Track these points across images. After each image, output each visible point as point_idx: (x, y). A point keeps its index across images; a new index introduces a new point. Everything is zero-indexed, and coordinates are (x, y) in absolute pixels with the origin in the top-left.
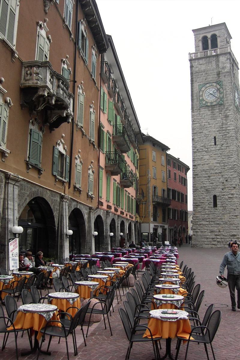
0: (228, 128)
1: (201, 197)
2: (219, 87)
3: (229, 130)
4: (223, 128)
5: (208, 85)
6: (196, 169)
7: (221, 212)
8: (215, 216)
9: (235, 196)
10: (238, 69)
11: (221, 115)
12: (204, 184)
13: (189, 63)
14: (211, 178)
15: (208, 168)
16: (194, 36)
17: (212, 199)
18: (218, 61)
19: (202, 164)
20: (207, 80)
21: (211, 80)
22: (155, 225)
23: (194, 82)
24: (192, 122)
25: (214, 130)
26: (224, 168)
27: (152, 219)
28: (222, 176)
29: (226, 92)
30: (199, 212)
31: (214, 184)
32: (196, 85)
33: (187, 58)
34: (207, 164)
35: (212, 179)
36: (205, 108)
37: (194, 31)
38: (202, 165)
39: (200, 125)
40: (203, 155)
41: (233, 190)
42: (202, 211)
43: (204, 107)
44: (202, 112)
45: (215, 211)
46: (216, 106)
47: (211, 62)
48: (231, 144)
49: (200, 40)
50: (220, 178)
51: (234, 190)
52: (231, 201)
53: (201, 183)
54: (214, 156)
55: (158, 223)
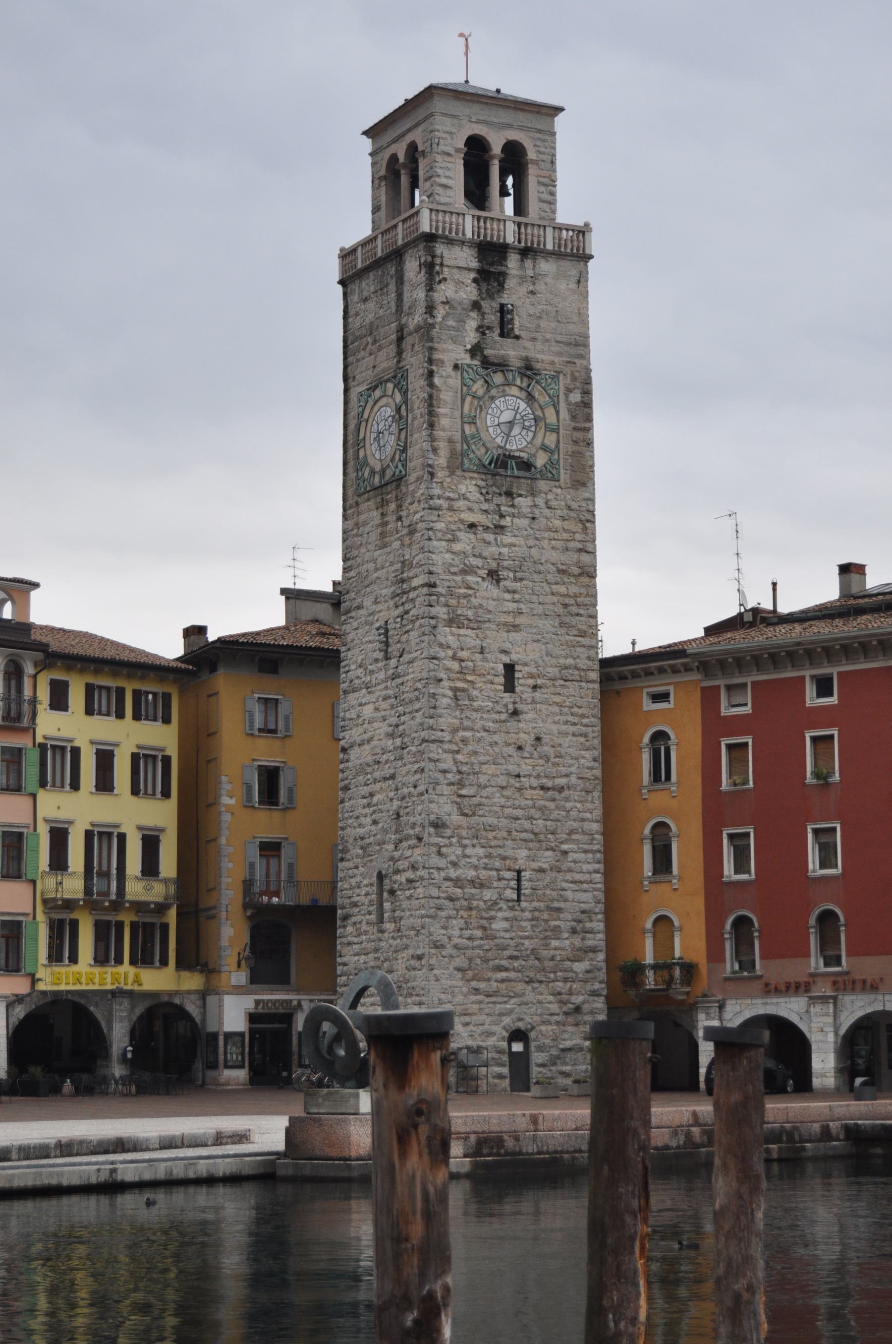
0: (416, 582)
1: (353, 881)
2: (398, 398)
3: (415, 589)
4: (403, 581)
5: (378, 393)
6: (346, 764)
7: (391, 941)
8: (378, 958)
9: (419, 873)
10: (591, 257)
11: (400, 523)
12: (360, 825)
13: (340, 289)
14: (375, 799)
15: (369, 759)
16: (369, 160)
17: (374, 888)
18: (400, 279)
19: (358, 740)
20: (377, 370)
21: (384, 371)
22: (257, 1002)
23: (351, 383)
24: (344, 561)
25: (384, 592)
26: (401, 758)
27: (240, 977)
28: (397, 789)
29: (414, 419)
30: (349, 944)
31: (380, 825)
32: (353, 396)
33: (333, 270)
34: (369, 741)
35: (376, 805)
36: (368, 500)
37: (365, 133)
38: (359, 745)
39: (359, 573)
40: (361, 705)
41: (417, 847)
42: (356, 940)
43: (366, 495)
44: (362, 518)
45: (380, 940)
46: (389, 488)
47: (387, 285)
48: (419, 652)
49: (381, 178)
50: (391, 800)
51: (418, 851)
52: (411, 896)
53: (355, 824)
54: (384, 705)
55: (298, 991)
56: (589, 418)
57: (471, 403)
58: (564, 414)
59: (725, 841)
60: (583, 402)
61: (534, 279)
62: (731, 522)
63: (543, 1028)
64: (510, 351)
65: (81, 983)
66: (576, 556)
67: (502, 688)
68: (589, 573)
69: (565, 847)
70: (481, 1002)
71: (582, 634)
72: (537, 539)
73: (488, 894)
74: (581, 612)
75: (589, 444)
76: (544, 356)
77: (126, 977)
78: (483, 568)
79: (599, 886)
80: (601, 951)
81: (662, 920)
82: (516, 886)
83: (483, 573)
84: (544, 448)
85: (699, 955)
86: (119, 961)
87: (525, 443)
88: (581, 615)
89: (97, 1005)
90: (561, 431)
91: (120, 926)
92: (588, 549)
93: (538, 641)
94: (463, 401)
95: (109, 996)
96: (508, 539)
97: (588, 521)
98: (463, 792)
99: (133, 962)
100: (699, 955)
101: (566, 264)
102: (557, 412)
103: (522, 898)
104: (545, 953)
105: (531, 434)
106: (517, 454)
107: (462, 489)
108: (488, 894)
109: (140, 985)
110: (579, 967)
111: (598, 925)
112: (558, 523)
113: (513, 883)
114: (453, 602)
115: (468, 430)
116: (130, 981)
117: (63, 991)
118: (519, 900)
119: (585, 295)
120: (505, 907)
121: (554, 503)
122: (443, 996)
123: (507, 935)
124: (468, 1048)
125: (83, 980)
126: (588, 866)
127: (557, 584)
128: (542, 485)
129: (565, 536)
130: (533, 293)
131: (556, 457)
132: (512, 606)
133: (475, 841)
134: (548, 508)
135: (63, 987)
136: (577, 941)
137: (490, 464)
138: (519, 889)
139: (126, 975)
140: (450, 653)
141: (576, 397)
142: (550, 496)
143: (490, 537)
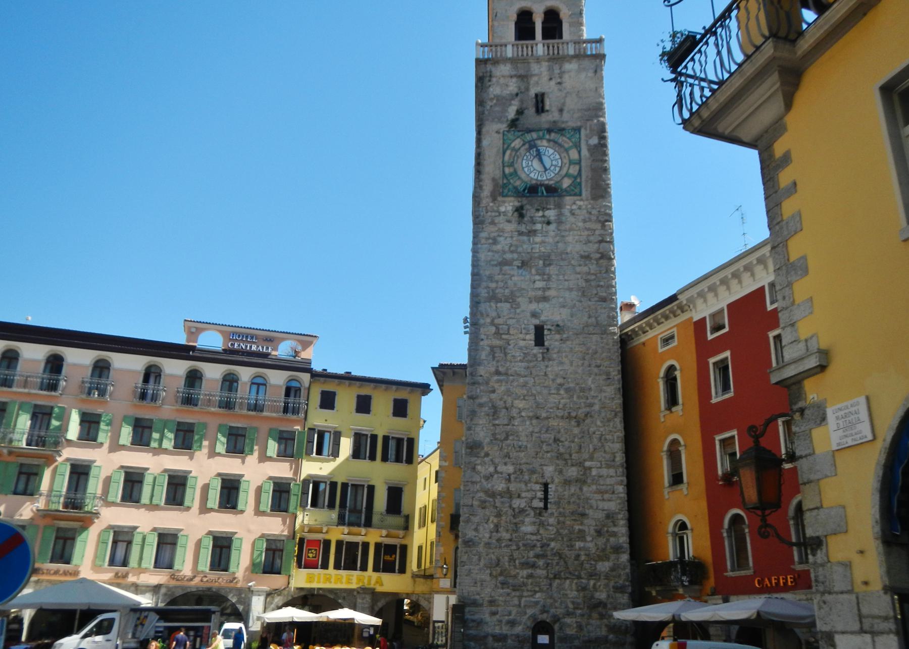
56: (605, 154)
57: (511, 155)
58: (585, 152)
59: (718, 447)
60: (599, 143)
61: (561, 75)
62: (738, 214)
63: (568, 620)
64: (545, 119)
65: (342, 583)
66: (597, 245)
67: (533, 343)
68: (606, 257)
69: (587, 464)
70: (508, 594)
71: (604, 300)
72: (563, 236)
73: (516, 503)
74: (602, 283)
75: (606, 170)
76: (570, 120)
77: (369, 581)
78: (517, 260)
79: (622, 495)
80: (624, 552)
81: (683, 526)
82: (542, 496)
83: (518, 263)
84: (567, 175)
85: (707, 555)
86: (364, 568)
87: (553, 175)
88: (602, 286)
89: (344, 598)
90: (583, 164)
91: (366, 545)
92: (606, 240)
93: (564, 307)
94: (504, 153)
95: (355, 593)
96: (538, 239)
97: (607, 221)
98: (497, 422)
99: (376, 569)
100: (707, 555)
101: (586, 63)
102: (579, 152)
103: (549, 506)
104: (570, 554)
105: (558, 169)
106: (546, 182)
107: (502, 209)
108: (516, 503)
109: (382, 585)
110: (604, 567)
111: (622, 529)
112: (580, 224)
113: (540, 494)
114: (493, 285)
115: (507, 170)
116: (373, 582)
117: (314, 589)
118: (546, 508)
119: (601, 79)
120: (532, 514)
121: (577, 212)
122: (472, 589)
123: (534, 537)
124: (494, 636)
125: (333, 580)
126: (614, 480)
127: (580, 265)
128: (568, 199)
129: (586, 233)
130: (560, 83)
131: (578, 180)
132: (540, 284)
133: (507, 460)
134: (573, 214)
135: (315, 585)
136: (601, 541)
137: (524, 190)
138: (546, 499)
139: (370, 577)
140: (488, 320)
141: (594, 141)
142: (574, 207)
143: (525, 238)
